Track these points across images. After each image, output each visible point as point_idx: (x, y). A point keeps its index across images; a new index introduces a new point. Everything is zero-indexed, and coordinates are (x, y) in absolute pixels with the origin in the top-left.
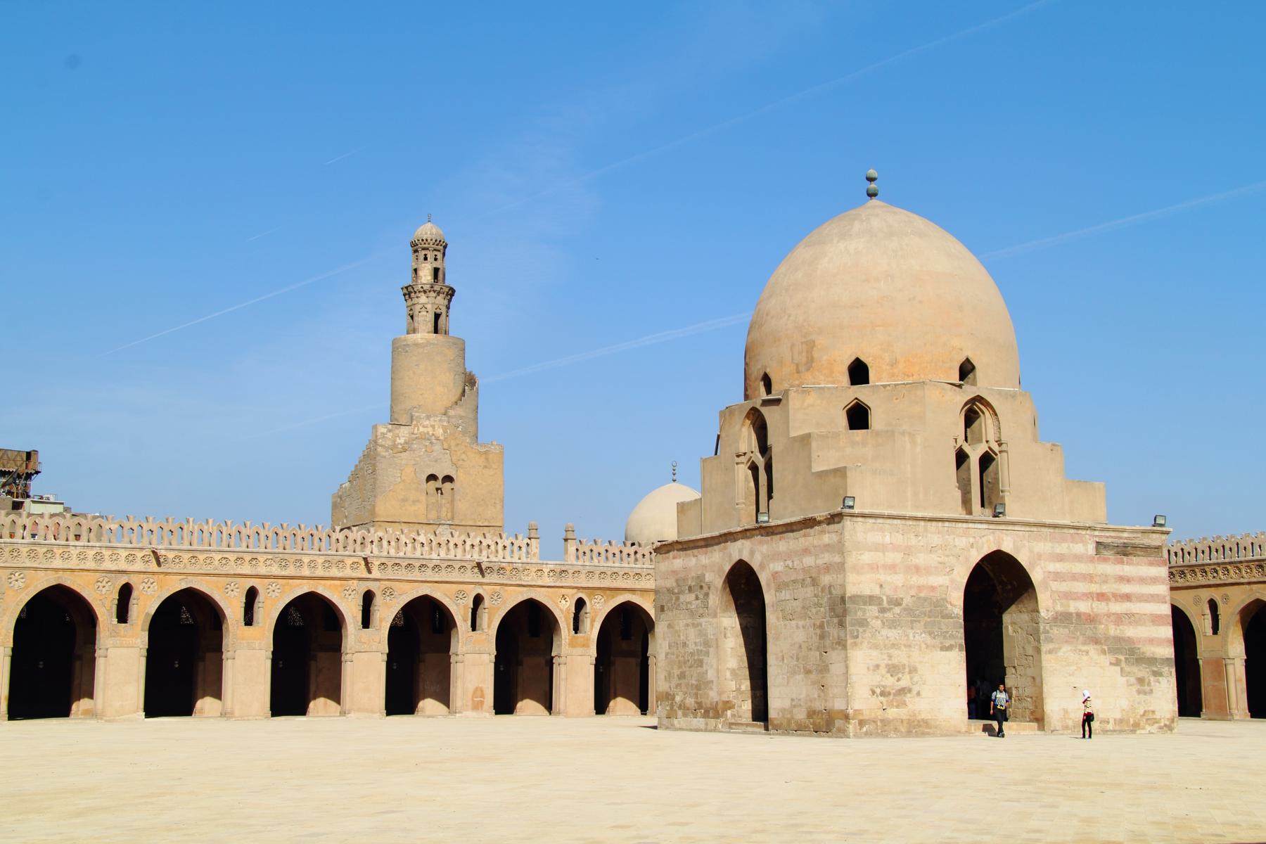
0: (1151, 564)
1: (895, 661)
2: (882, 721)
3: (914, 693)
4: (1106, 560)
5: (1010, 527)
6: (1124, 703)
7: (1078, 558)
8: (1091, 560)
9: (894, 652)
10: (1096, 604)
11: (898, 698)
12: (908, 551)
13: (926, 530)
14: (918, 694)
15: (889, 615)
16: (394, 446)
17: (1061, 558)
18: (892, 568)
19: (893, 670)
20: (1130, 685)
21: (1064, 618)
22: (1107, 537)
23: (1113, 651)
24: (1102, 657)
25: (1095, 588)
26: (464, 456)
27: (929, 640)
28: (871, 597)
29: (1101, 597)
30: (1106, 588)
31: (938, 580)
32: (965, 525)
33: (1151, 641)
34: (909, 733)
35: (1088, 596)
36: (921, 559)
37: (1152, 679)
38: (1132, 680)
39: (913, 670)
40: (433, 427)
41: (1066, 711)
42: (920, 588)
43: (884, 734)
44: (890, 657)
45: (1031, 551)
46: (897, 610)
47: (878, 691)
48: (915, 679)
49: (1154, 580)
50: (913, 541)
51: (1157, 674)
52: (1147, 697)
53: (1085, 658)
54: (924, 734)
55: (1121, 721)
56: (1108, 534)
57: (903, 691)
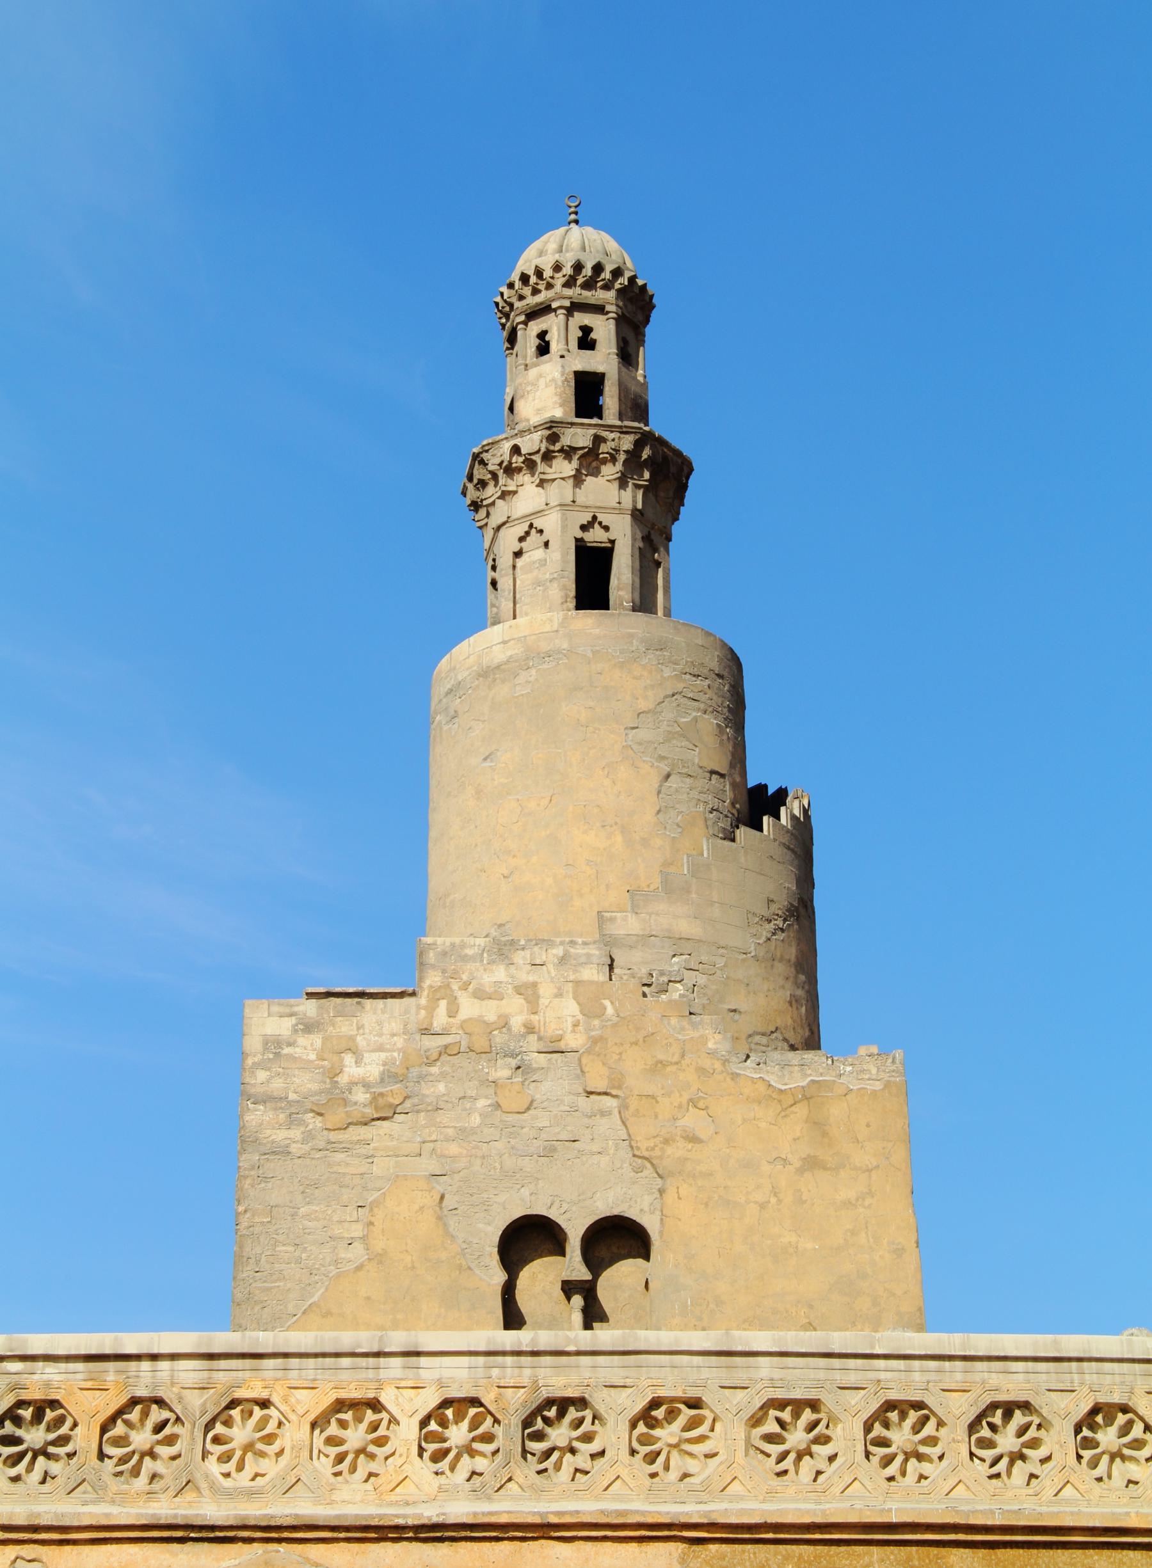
16: (334, 1095)
26: (692, 1120)
40: (529, 992)
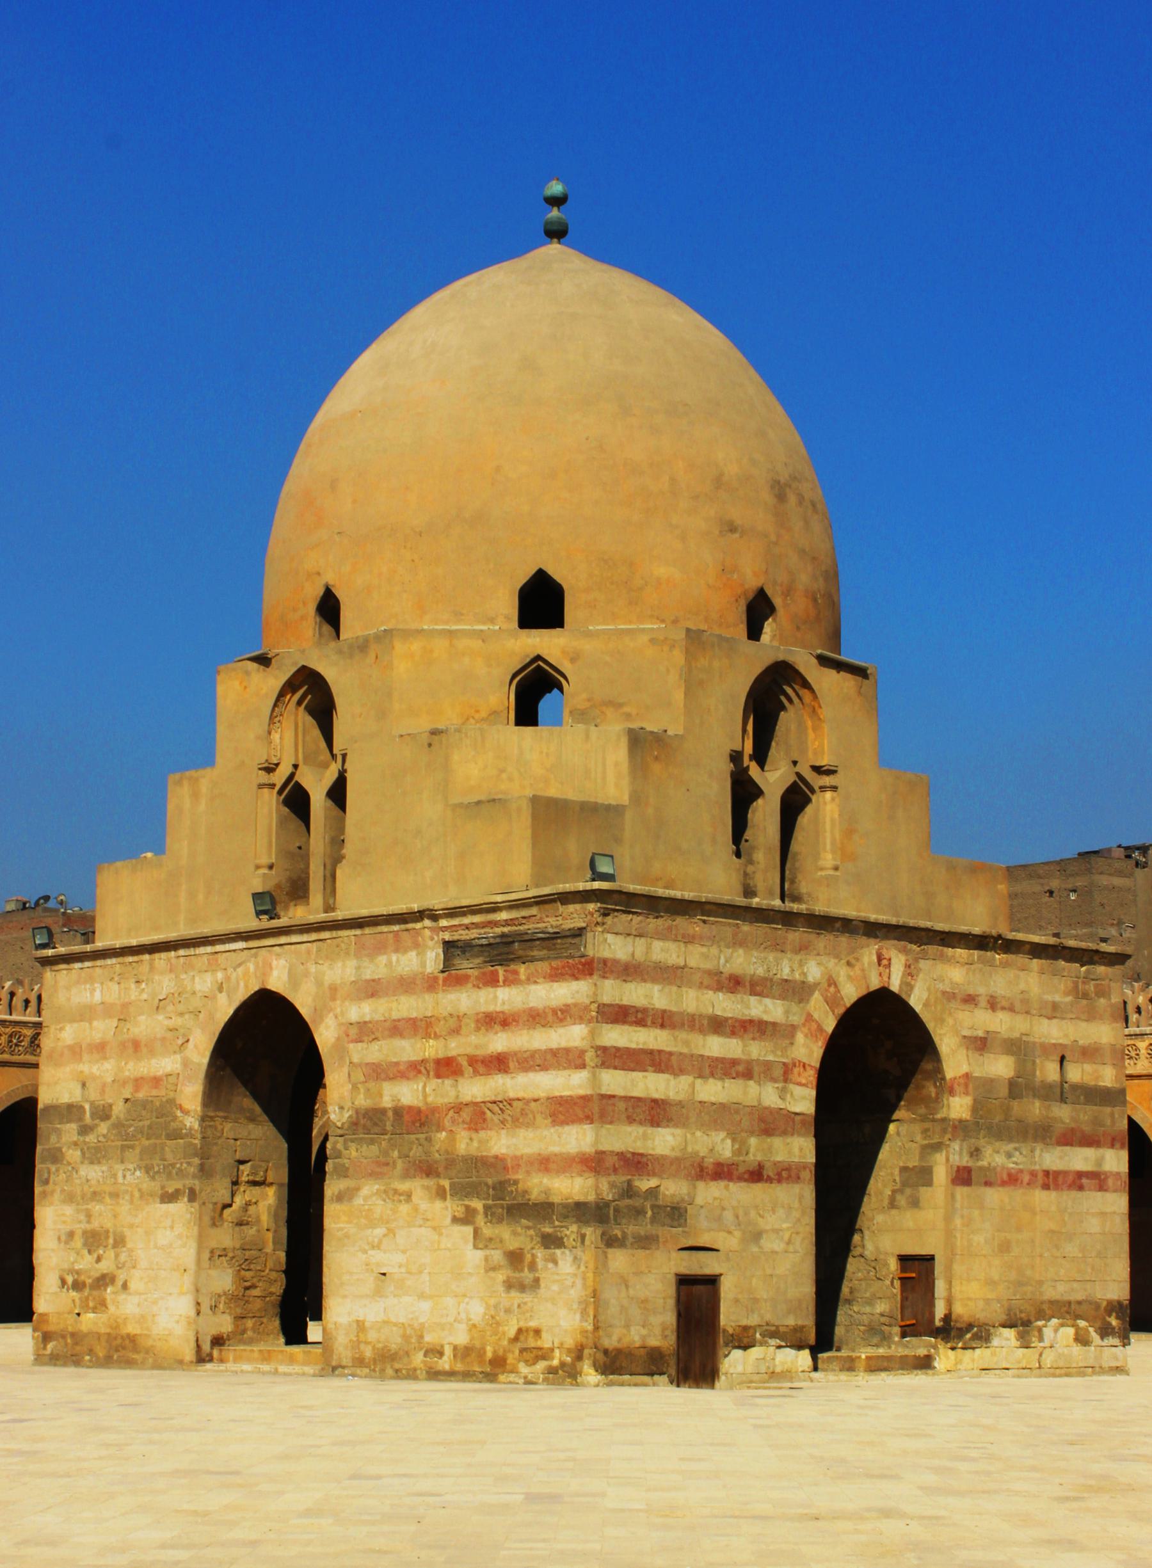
0: (556, 976)
1: (95, 1225)
2: (73, 1335)
3: (119, 1283)
4: (461, 981)
5: (283, 940)
6: (477, 1310)
7: (406, 985)
8: (431, 984)
9: (97, 1208)
10: (434, 1083)
11: (95, 1293)
12: (123, 1014)
13: (152, 968)
14: (125, 1286)
15: (91, 1138)
17: (371, 990)
18: (100, 1048)
19: (94, 1240)
20: (491, 1268)
21: (370, 1122)
22: (467, 929)
23: (462, 1190)
24: (439, 1204)
25: (431, 1049)
27: (147, 1184)
28: (70, 1107)
29: (446, 1067)
30: (455, 1047)
31: (166, 1064)
32: (209, 949)
33: (545, 1163)
34: (107, 1362)
35: (415, 1069)
36: (144, 1026)
37: (540, 1253)
38: (497, 1256)
39: (120, 1242)
41: (360, 1326)
42: (138, 1082)
43: (77, 1361)
44: (89, 1216)
45: (319, 983)
46: (103, 1128)
47: (70, 1280)
48: (123, 1257)
49: (562, 1015)
50: (134, 993)
51: (552, 1242)
52: (527, 1297)
53: (404, 1208)
54: (129, 1363)
55: (464, 1352)
56: (467, 920)
57: (104, 1280)
